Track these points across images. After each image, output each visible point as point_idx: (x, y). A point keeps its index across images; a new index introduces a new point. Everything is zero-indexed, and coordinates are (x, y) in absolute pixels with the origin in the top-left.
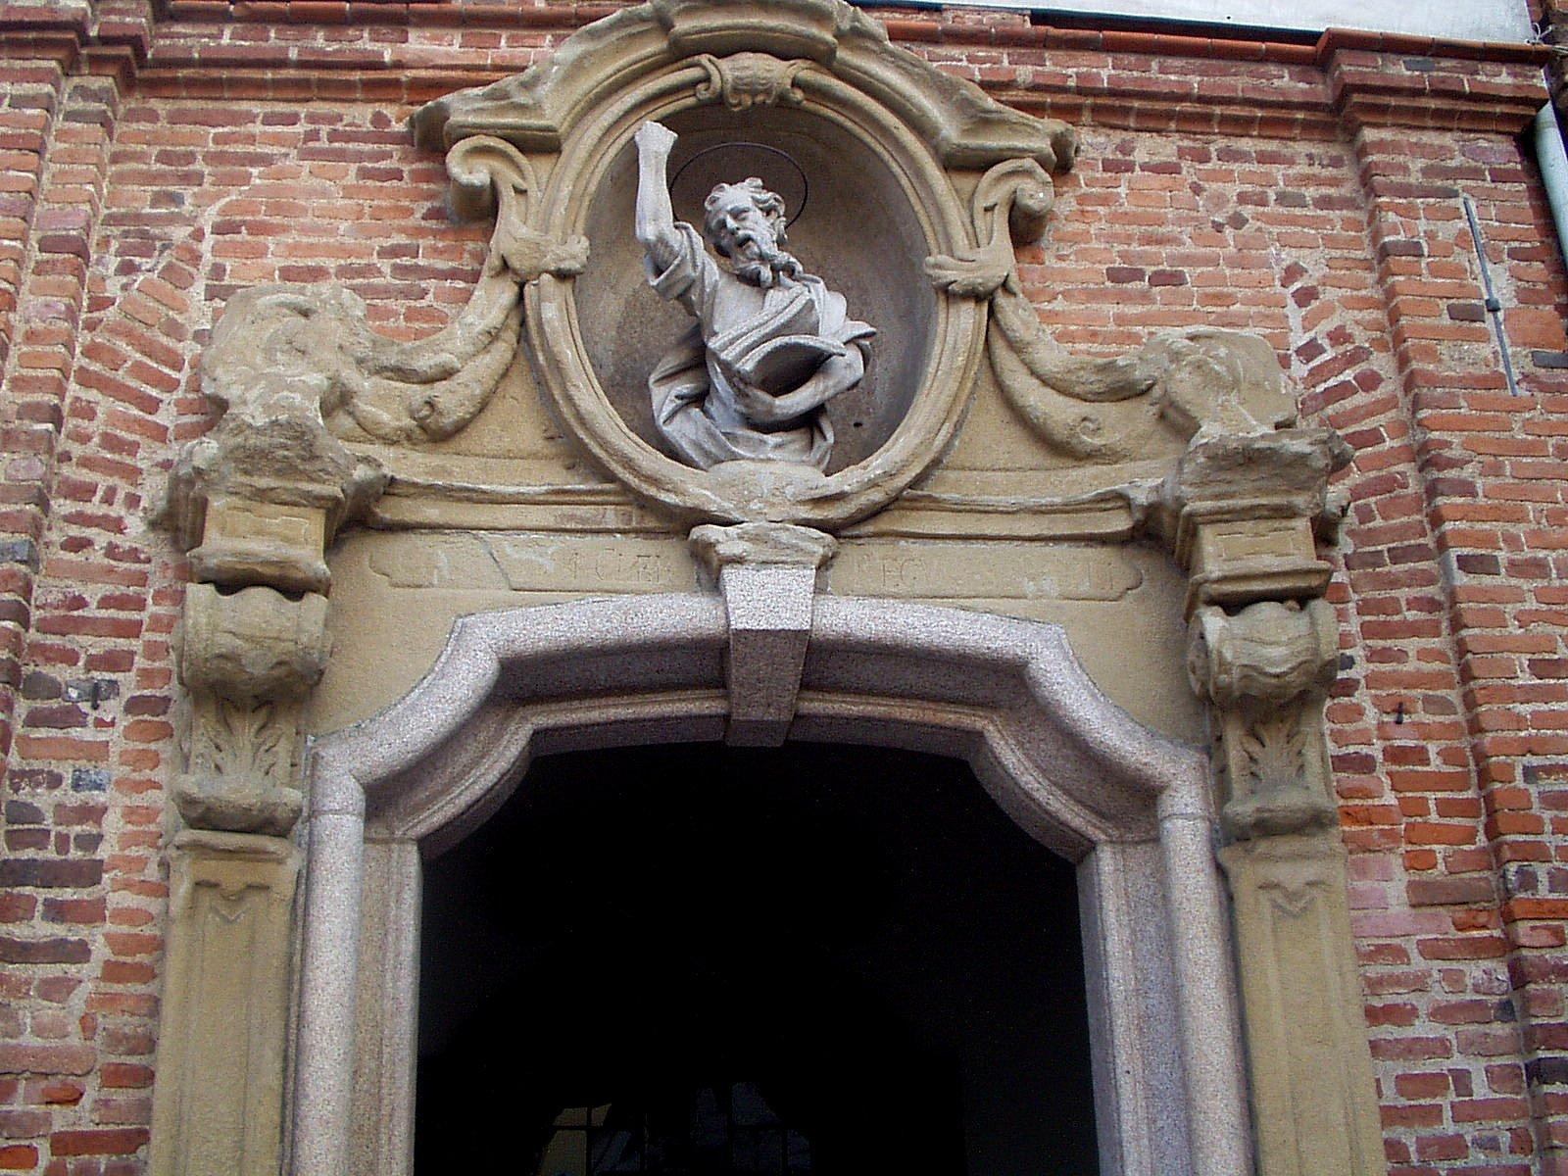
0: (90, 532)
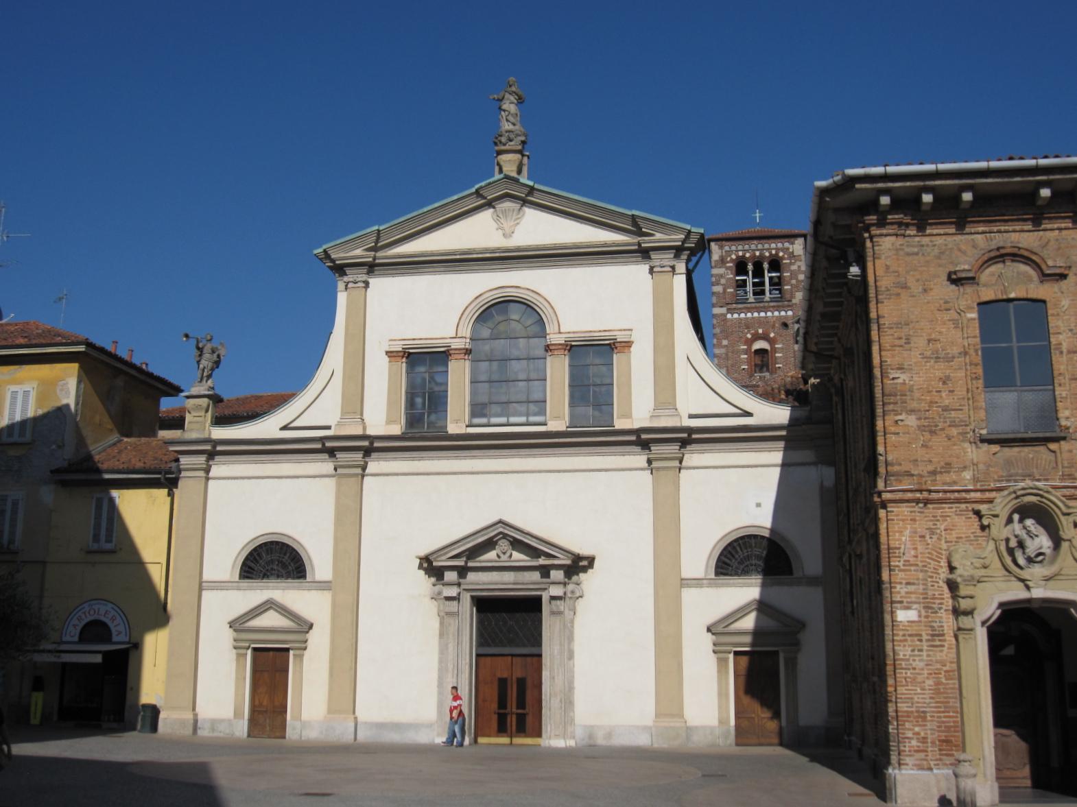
0: (934, 584)
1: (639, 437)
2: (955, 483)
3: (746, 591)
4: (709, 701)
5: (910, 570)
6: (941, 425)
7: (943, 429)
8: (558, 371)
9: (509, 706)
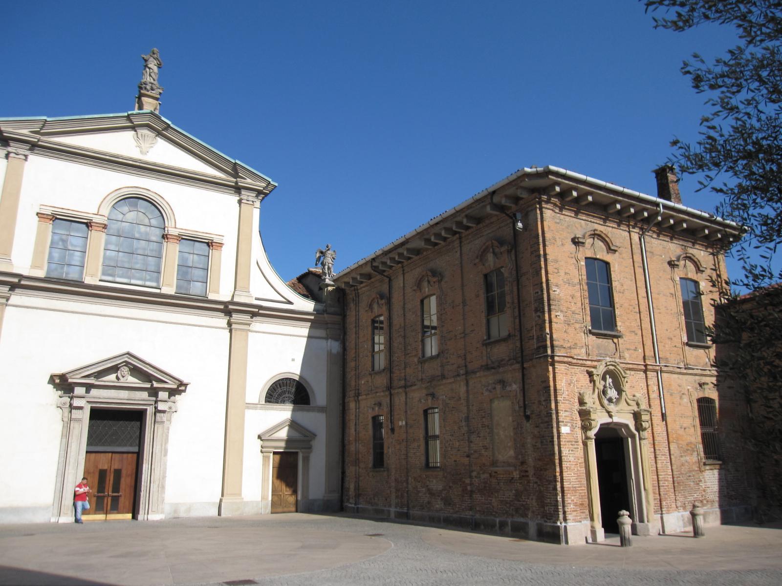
1: (226, 307)
2: (579, 355)
3: (282, 413)
4: (256, 484)
5: (565, 403)
6: (572, 322)
7: (573, 324)
8: (172, 253)
9: (106, 490)
